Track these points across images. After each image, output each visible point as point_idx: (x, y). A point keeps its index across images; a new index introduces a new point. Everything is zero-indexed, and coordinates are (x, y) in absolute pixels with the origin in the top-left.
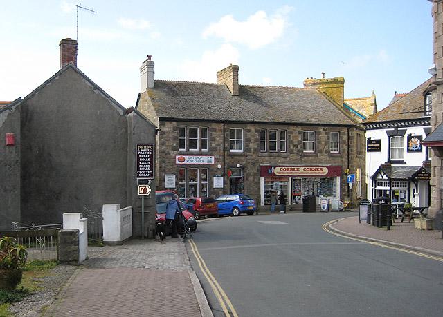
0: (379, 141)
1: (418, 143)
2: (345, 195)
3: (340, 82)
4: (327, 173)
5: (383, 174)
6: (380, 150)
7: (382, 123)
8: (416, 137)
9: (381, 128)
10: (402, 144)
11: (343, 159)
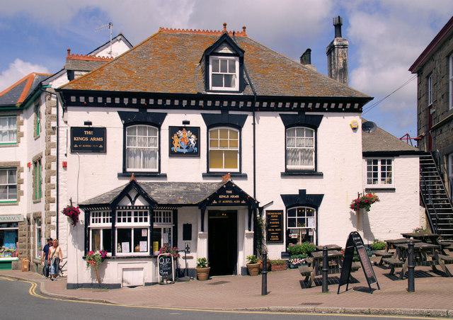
0: (102, 132)
1: (192, 140)
5: (133, 195)
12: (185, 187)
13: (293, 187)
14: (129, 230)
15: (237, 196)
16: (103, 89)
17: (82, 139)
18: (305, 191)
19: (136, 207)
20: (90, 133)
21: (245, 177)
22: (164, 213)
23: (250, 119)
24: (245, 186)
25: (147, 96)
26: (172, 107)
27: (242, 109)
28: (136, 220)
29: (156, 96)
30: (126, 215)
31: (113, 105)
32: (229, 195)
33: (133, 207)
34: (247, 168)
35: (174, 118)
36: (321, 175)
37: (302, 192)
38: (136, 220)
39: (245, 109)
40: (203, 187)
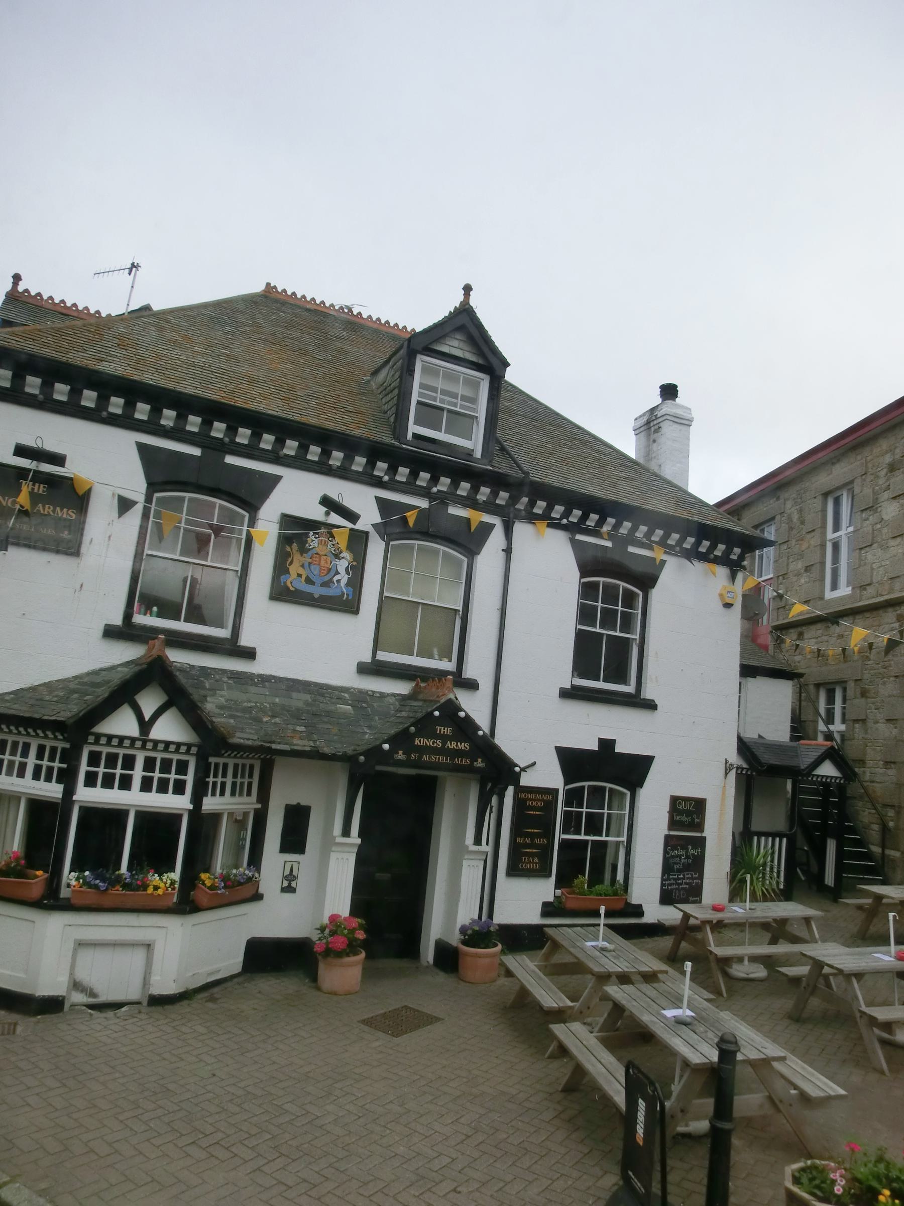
1: (342, 565)
9: (113, 421)
12: (308, 697)
14: (116, 816)
15: (464, 746)
18: (612, 742)
19: (156, 743)
21: (472, 685)
22: (236, 766)
26: (299, 463)
28: (146, 785)
31: (125, 422)
32: (444, 738)
33: (144, 740)
36: (651, 706)
37: (607, 745)
38: (146, 785)
39: (490, 507)
40: (360, 698)
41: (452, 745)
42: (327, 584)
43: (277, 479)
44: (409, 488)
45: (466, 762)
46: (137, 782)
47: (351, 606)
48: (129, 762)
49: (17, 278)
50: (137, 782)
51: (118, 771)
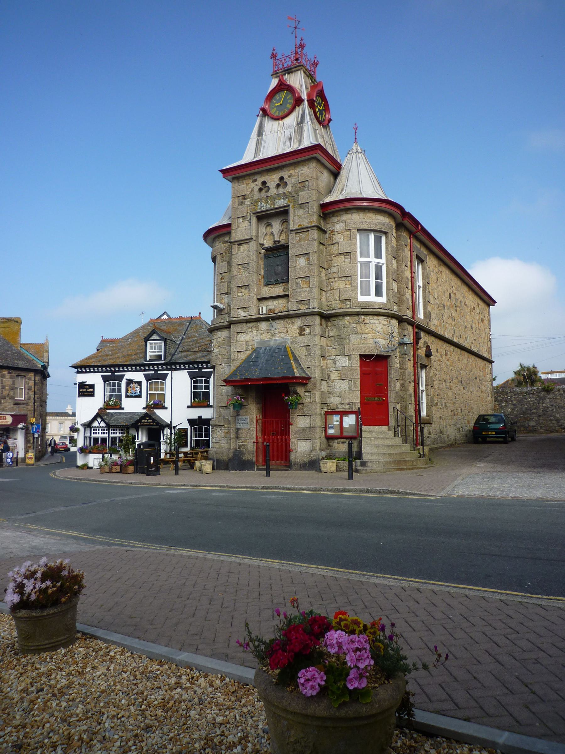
0: (92, 386)
1: (138, 389)
2: (30, 447)
3: (17, 322)
4: (9, 423)
6: (93, 396)
7: (98, 367)
8: (136, 382)
9: (95, 372)
10: (119, 390)
11: (29, 407)
13: (195, 413)
14: (98, 439)
15: (151, 421)
16: (92, 364)
17: (83, 390)
20: (87, 387)
23: (169, 377)
24: (162, 414)
25: (114, 366)
26: (128, 371)
27: (164, 370)
29: (119, 366)
30: (97, 430)
32: (147, 420)
34: (168, 404)
35: (129, 375)
37: (200, 417)
38: (102, 433)
41: (149, 421)
42: (135, 393)
43: (124, 375)
44: (149, 370)
45: (152, 424)
46: (100, 433)
47: (140, 396)
48: (99, 430)
49: (102, 337)
50: (100, 433)
51: (97, 431)
